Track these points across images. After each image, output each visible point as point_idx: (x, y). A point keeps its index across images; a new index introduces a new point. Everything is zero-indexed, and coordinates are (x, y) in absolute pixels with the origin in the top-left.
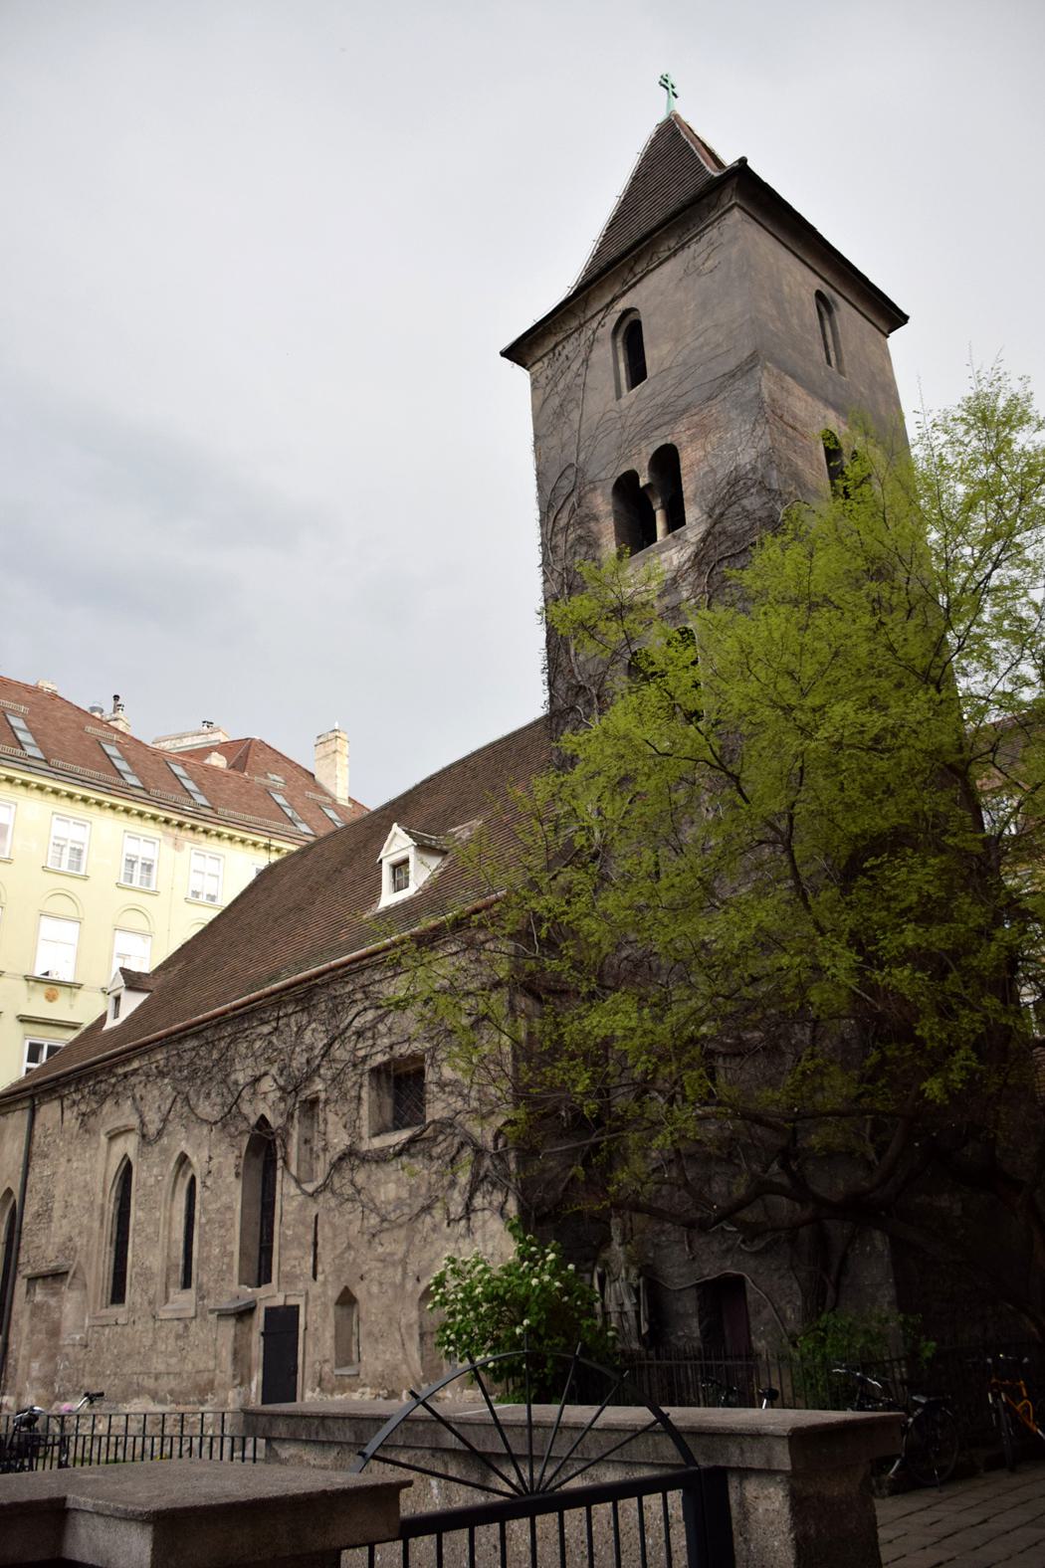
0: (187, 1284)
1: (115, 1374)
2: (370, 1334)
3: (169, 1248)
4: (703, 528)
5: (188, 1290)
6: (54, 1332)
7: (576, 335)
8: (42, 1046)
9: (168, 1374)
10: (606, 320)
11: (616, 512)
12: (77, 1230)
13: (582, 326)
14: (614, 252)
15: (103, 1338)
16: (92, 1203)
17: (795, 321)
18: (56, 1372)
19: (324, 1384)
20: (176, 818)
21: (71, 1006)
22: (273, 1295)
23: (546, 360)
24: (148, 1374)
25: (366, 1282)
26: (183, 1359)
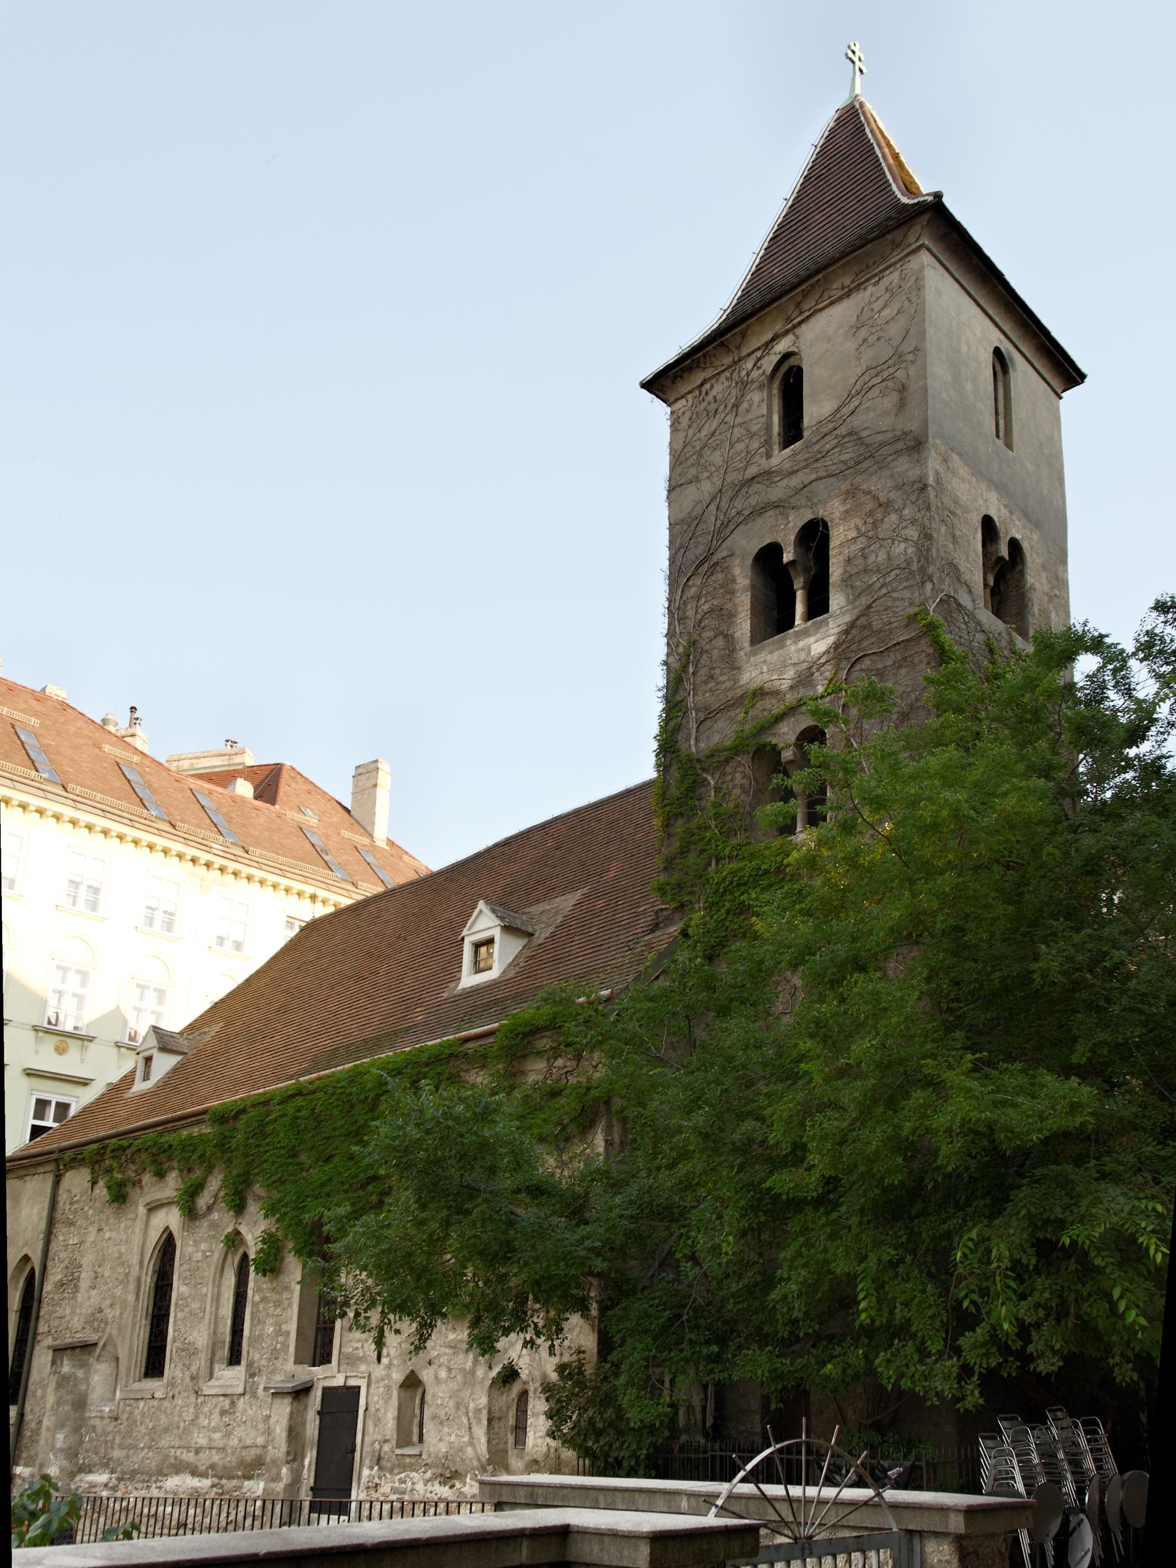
0: (234, 1358)
1: (149, 1448)
2: (435, 1417)
3: (216, 1324)
4: (848, 618)
5: (237, 1368)
6: (81, 1404)
7: (727, 374)
8: (48, 1103)
9: (210, 1448)
10: (762, 361)
11: (753, 587)
12: (108, 1302)
13: (735, 363)
14: (780, 274)
15: (137, 1411)
16: (127, 1275)
17: (969, 387)
18: (81, 1442)
19: (384, 1463)
20: (204, 857)
21: (82, 1061)
22: (332, 1376)
23: (690, 397)
24: (188, 1448)
25: (434, 1367)
26: (228, 1435)
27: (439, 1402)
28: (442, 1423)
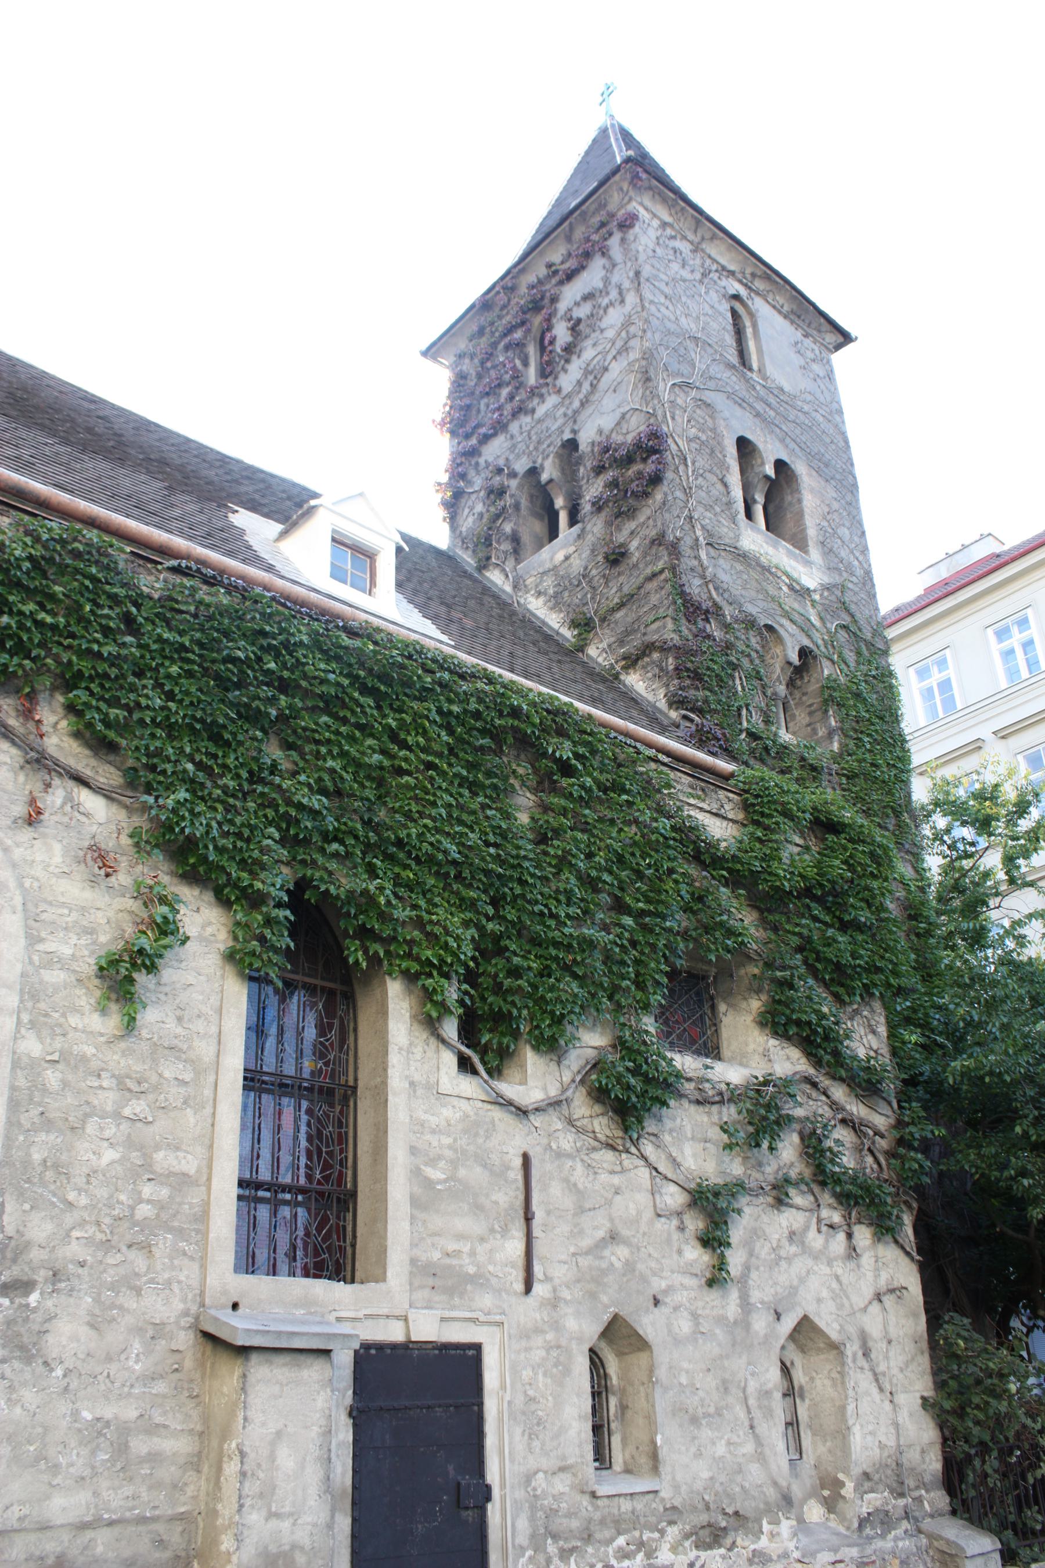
25: (664, 1310)
27: (684, 1380)
28: (695, 1420)
